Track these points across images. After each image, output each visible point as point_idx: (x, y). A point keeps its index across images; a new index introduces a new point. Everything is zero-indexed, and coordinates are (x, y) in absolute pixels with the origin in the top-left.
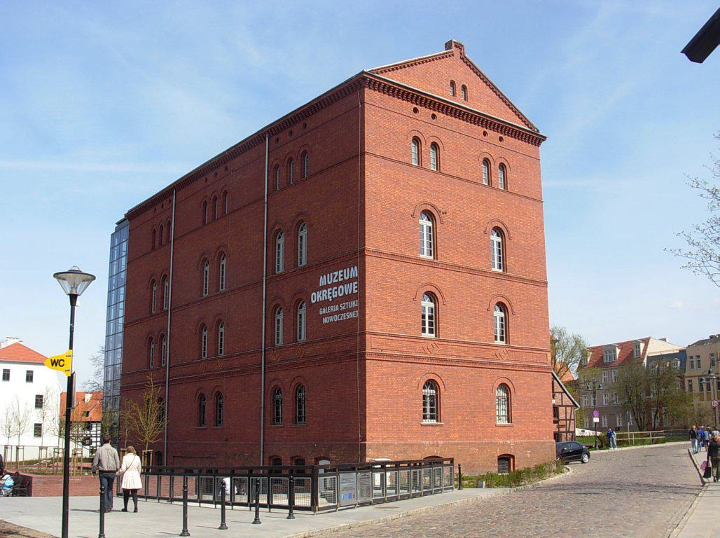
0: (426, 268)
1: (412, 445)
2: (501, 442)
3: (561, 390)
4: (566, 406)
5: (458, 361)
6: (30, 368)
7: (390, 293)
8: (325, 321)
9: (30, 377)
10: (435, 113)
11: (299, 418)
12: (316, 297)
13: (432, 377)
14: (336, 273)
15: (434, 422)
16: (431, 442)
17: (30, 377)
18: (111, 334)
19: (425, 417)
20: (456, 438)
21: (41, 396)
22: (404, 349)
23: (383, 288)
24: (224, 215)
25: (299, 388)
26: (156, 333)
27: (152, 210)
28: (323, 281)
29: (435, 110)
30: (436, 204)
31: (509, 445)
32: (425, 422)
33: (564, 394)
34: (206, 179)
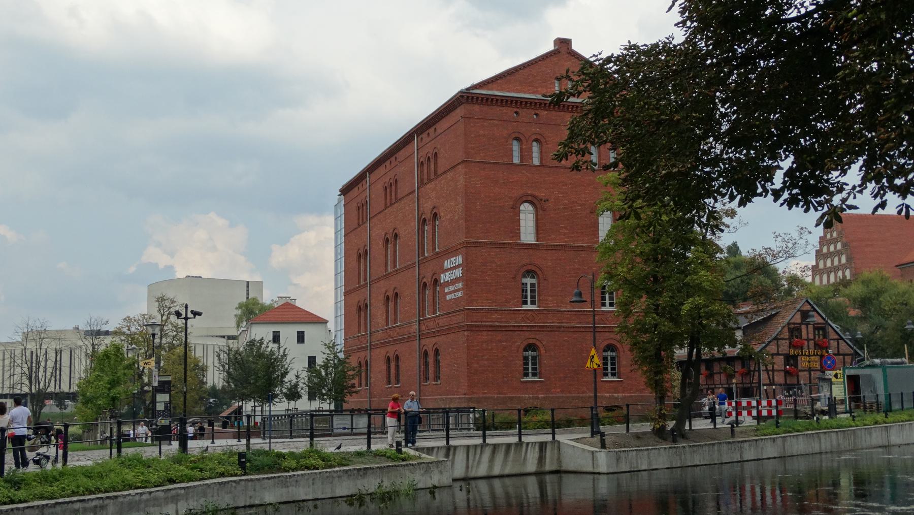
0: (526, 251)
1: (511, 399)
2: (607, 395)
3: (837, 337)
4: (844, 355)
5: (560, 327)
6: (301, 328)
7: (489, 275)
8: (449, 297)
9: (301, 338)
10: (536, 112)
11: (437, 378)
12: (444, 278)
13: (531, 341)
14: (452, 259)
15: (536, 379)
16: (531, 396)
17: (301, 338)
18: (339, 300)
19: (527, 375)
20: (558, 392)
21: (314, 357)
22: (503, 320)
23: (481, 272)
24: (397, 201)
25: (437, 352)
26: (362, 302)
27: (356, 189)
28: (447, 265)
29: (536, 109)
30: (537, 193)
31: (617, 398)
32: (526, 379)
33: (841, 341)
34: (396, 158)
